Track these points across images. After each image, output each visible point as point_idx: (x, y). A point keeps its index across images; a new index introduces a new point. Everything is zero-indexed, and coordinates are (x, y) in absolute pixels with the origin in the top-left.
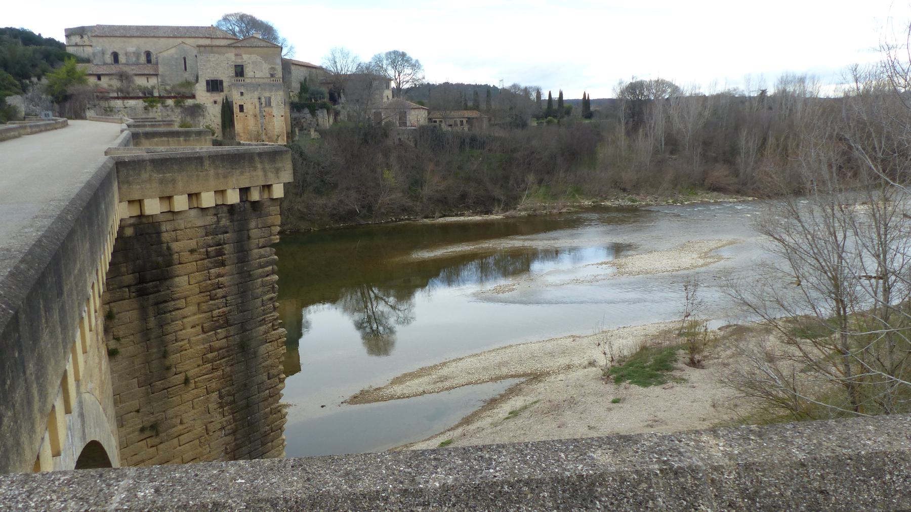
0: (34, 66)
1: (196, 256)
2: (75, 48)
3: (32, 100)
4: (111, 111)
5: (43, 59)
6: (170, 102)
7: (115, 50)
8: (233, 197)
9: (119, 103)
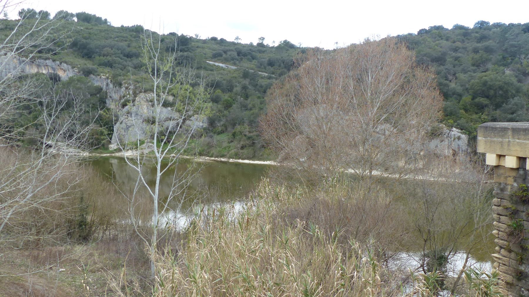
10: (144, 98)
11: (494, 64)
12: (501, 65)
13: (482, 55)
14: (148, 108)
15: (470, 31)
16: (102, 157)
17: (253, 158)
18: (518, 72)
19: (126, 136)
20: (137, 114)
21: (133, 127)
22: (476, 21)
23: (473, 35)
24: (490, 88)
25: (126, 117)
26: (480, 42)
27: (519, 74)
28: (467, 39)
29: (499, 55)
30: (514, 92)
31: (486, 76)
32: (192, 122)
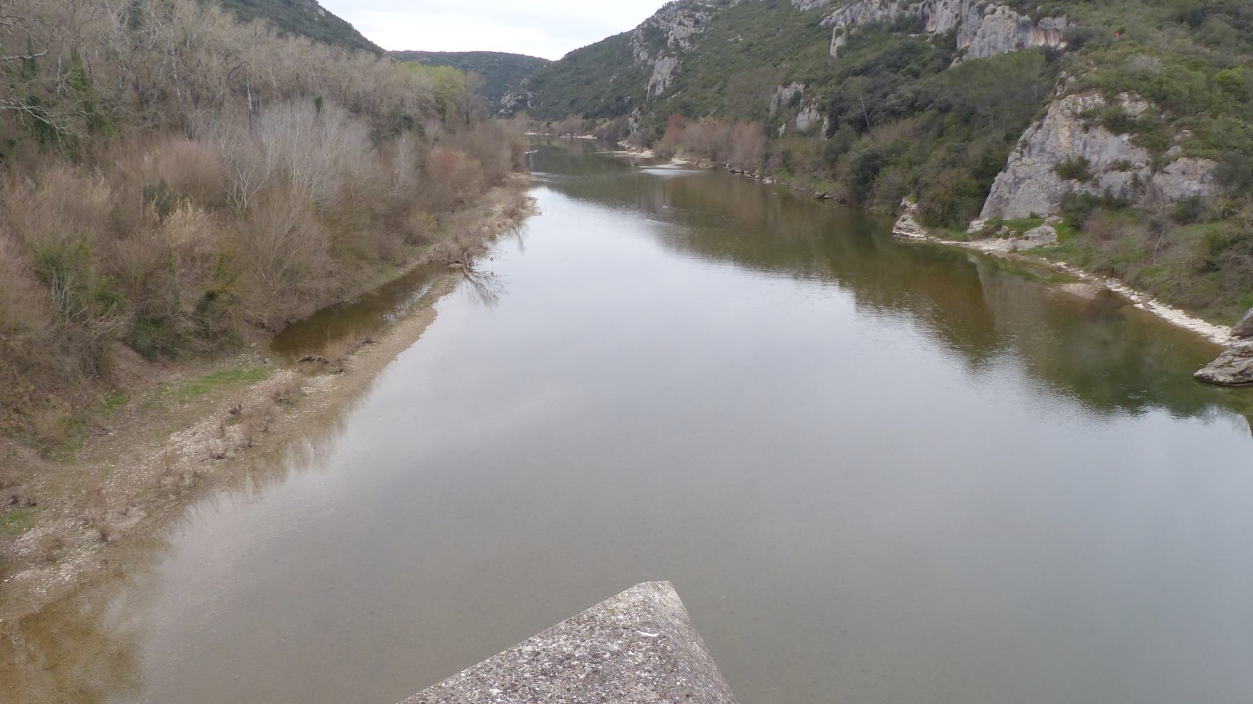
10: (1068, 109)
14: (1072, 134)
16: (942, 244)
17: (1194, 309)
19: (1012, 204)
20: (1042, 150)
21: (1028, 181)
25: (1019, 155)
32: (1167, 177)
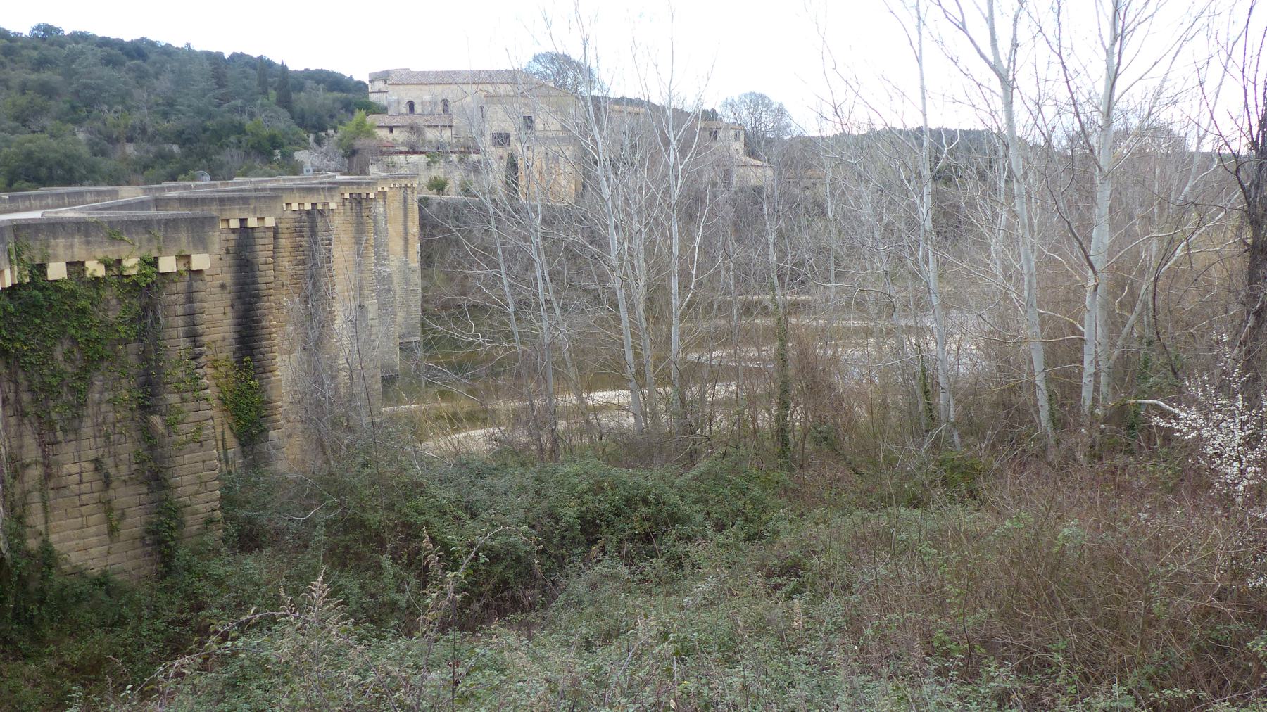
0: (332, 116)
1: (289, 231)
2: (378, 95)
3: (326, 155)
4: (393, 166)
5: (342, 109)
6: (454, 158)
7: (411, 99)
8: (308, 207)
9: (402, 157)
11: (55, 119)
12: (68, 121)
13: (32, 99)
15: (20, 44)
18: (99, 136)
22: (35, 24)
23: (25, 52)
24: (40, 163)
26: (38, 71)
27: (100, 139)
28: (12, 61)
29: (65, 102)
30: (84, 172)
31: (30, 141)
